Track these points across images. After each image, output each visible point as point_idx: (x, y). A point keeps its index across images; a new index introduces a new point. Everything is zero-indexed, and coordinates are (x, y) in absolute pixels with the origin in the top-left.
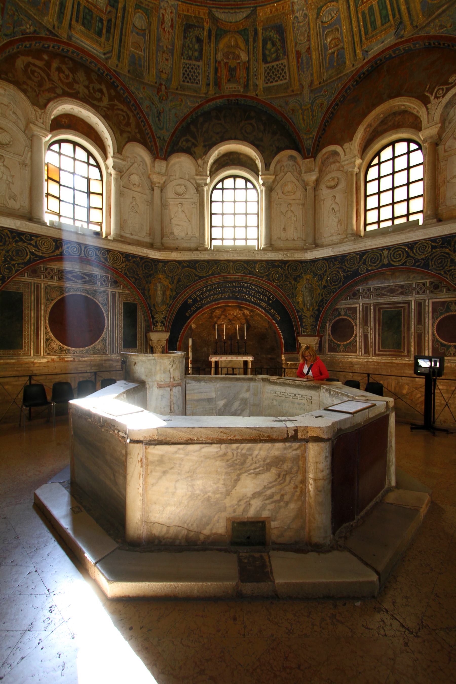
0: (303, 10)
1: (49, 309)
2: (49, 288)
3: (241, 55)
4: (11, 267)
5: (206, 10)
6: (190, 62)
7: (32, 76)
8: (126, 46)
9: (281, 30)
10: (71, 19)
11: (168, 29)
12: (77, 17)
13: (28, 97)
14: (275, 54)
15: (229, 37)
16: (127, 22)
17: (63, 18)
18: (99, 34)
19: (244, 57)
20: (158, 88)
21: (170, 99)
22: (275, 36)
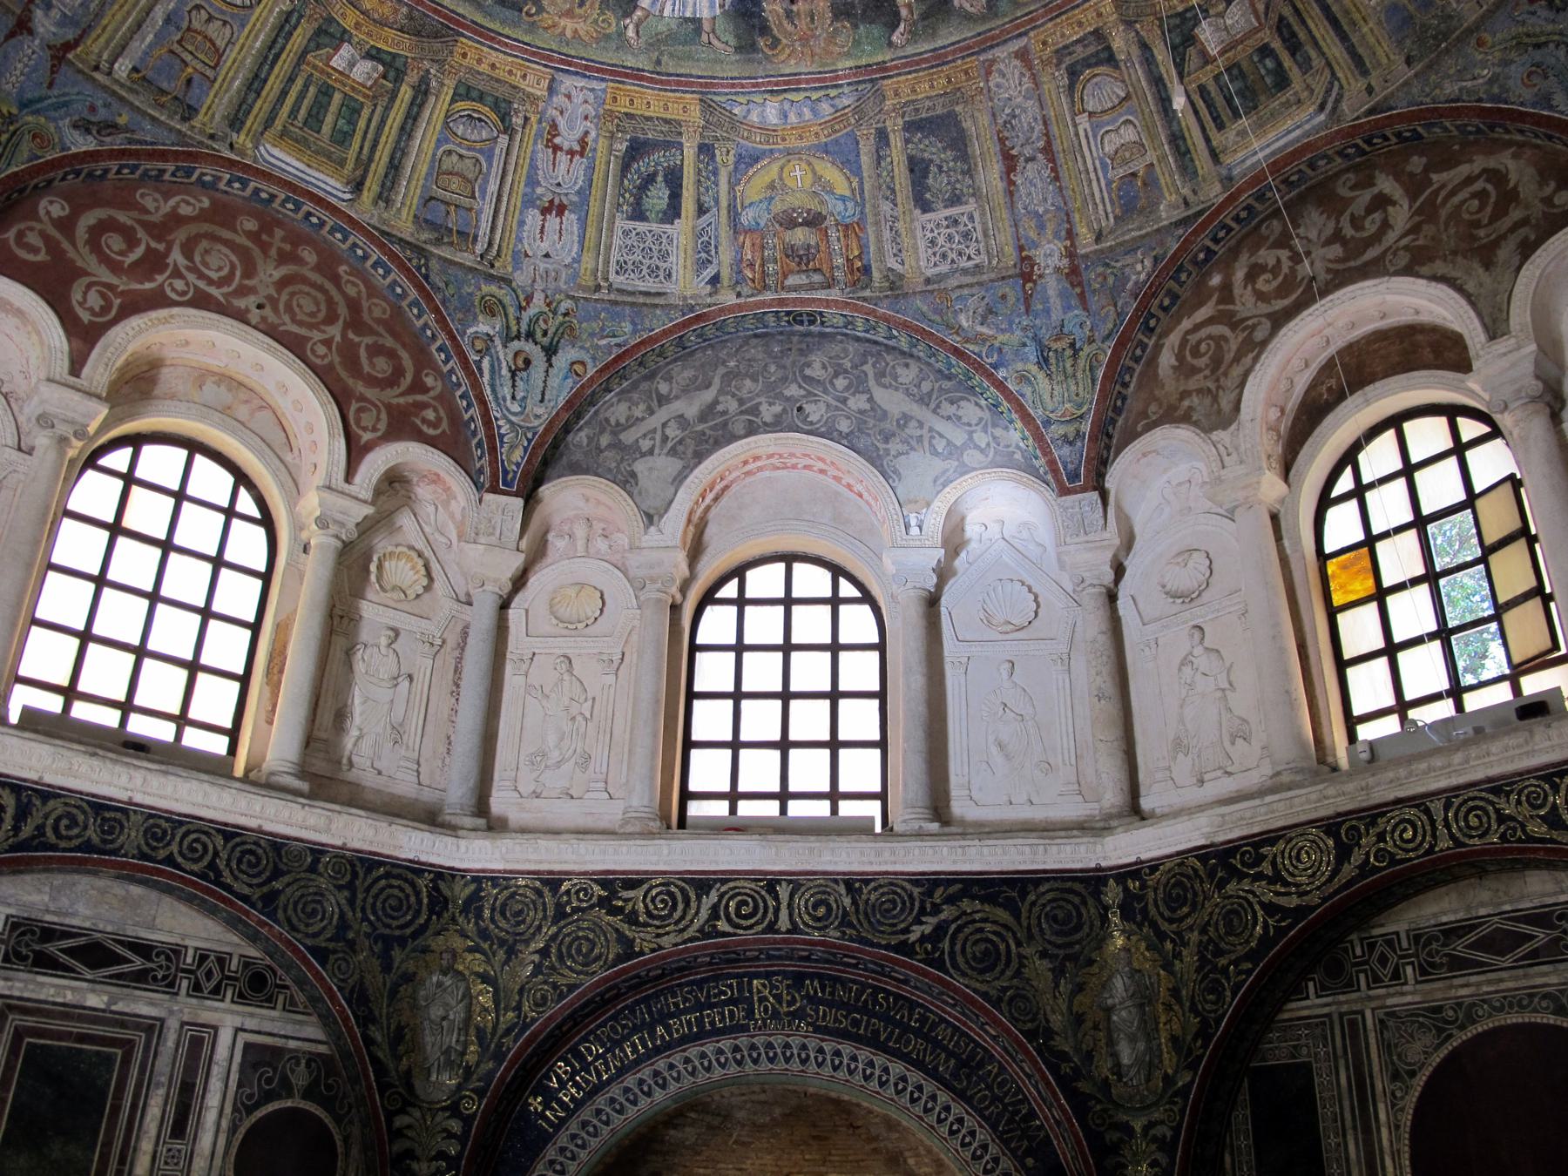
1: (1407, 1119)
2: (1390, 1024)
4: (1218, 981)
7: (1195, 362)
8: (1356, 16)
10: (1208, 140)
12: (1214, 120)
13: (1196, 424)
17: (1192, 160)
18: (1282, 81)
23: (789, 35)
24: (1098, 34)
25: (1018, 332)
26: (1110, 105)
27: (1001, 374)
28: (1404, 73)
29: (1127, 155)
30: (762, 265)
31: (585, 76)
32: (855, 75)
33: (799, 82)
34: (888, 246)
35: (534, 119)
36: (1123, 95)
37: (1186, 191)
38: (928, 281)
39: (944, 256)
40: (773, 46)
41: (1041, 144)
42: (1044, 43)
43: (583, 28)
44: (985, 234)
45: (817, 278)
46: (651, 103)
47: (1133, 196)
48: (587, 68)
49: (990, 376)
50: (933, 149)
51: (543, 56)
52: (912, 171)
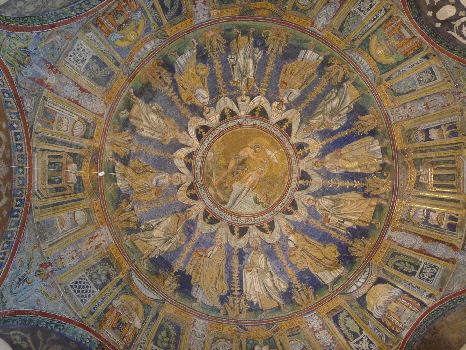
0: (202, 330)
3: (136, 320)
5: (128, 267)
6: (89, 281)
8: (56, 211)
9: (178, 330)
10: (49, 150)
11: (92, 244)
14: (167, 344)
15: (133, 298)
16: (73, 206)
17: (46, 142)
18: (51, 181)
19: (137, 323)
20: (46, 263)
21: (47, 283)
22: (172, 331)
23: (156, 69)
24: (92, 138)
25: (40, 50)
26: (74, 128)
27: (35, 33)
28: (37, 220)
29: (59, 124)
30: (127, 3)
31: (202, 23)
32: (135, 73)
33: (147, 60)
34: (95, 37)
35: (211, 3)
36: (74, 134)
37: (39, 135)
38: (77, 38)
39: (78, 49)
40: (158, 63)
41: (80, 102)
42: (100, 123)
43: (208, 35)
44: (72, 66)
45: (109, 11)
46: (181, 27)
47: (49, 117)
48: (202, 25)
49: (37, 29)
50: (102, 73)
51: (216, 21)
52: (104, 63)
